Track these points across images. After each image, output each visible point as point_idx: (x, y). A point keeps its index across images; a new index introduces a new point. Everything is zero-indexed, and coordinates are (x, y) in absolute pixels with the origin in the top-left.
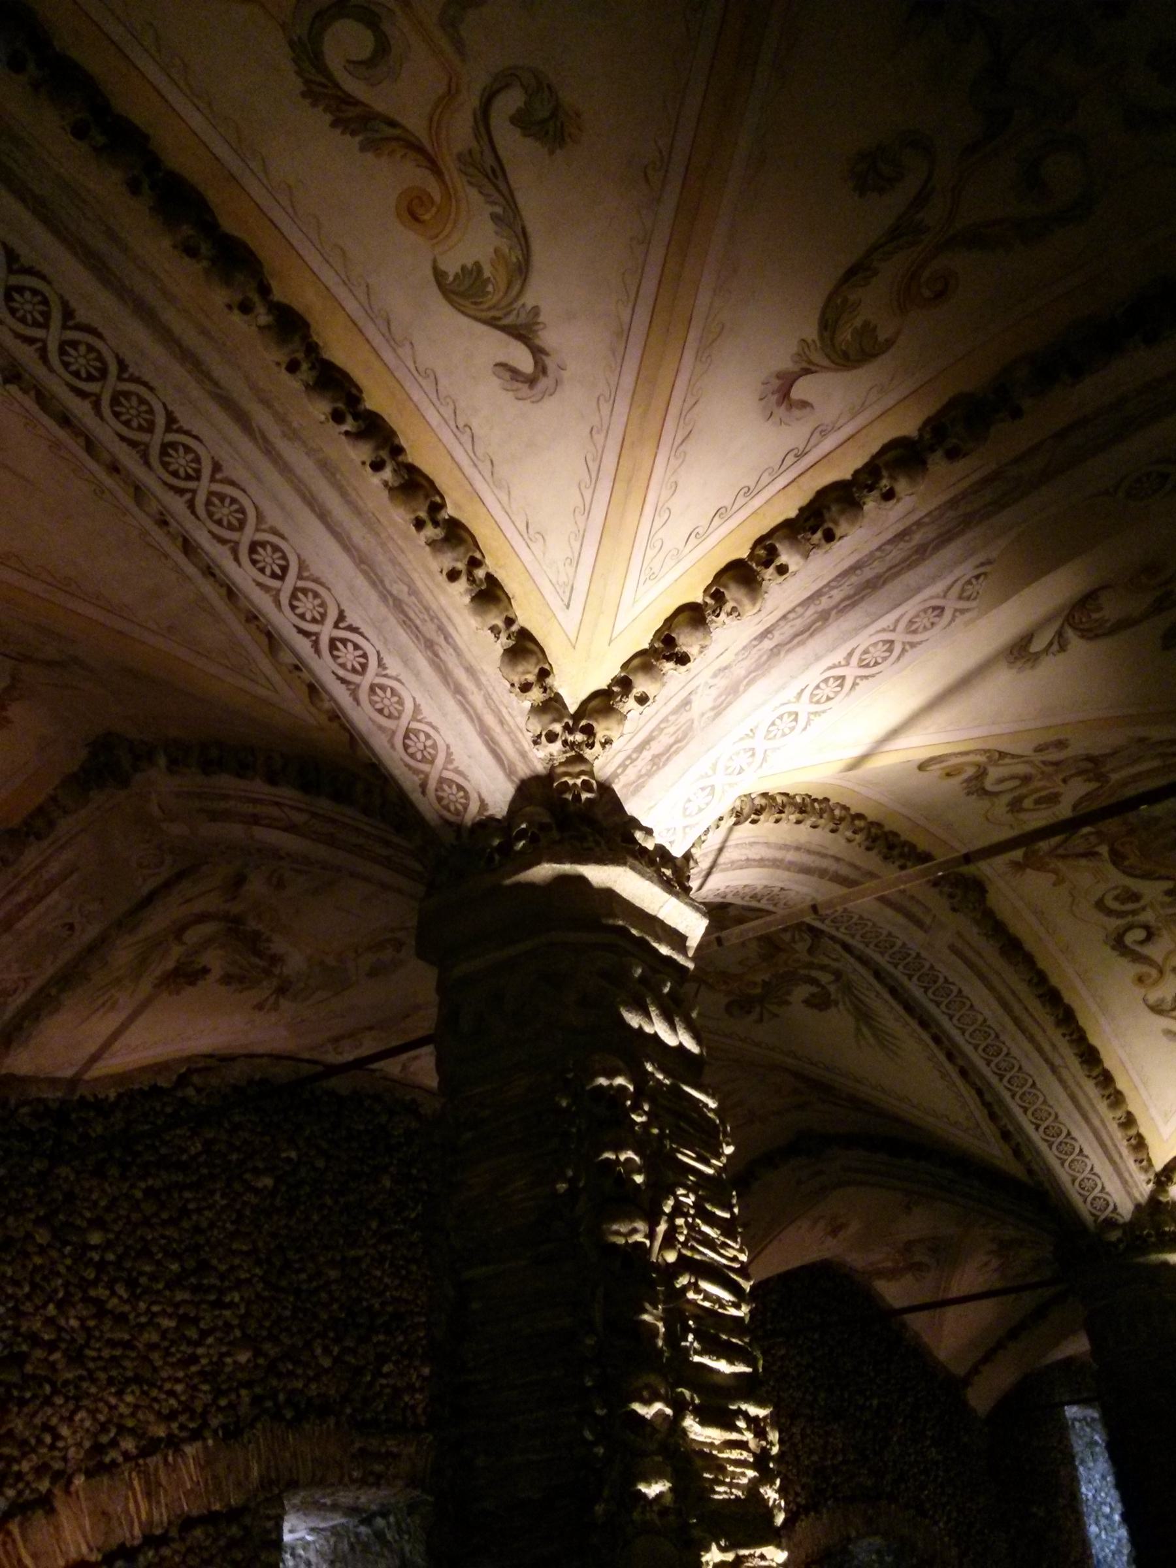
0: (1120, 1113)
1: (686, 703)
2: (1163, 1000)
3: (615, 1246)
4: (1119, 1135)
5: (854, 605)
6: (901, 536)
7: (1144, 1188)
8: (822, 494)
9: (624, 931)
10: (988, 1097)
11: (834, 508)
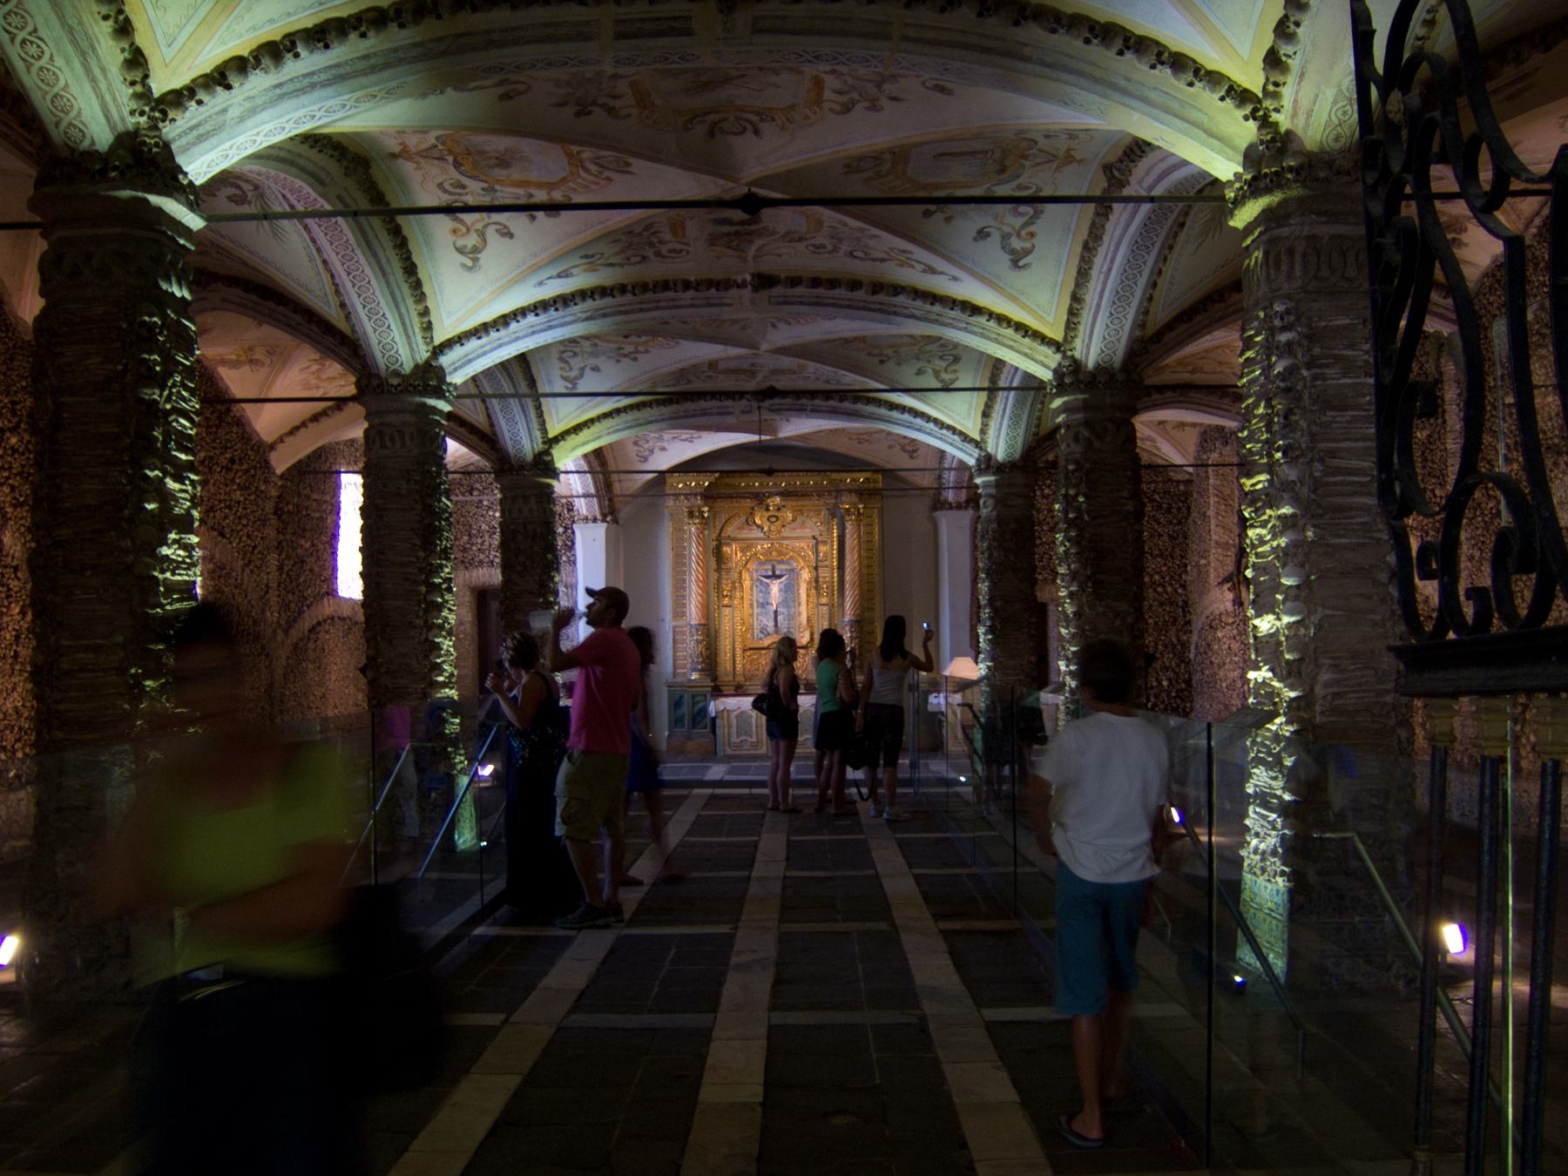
0: (420, 308)
1: (225, 110)
2: (465, 246)
3: (144, 399)
4: (416, 319)
5: (330, 85)
6: (365, 57)
7: (423, 354)
8: (328, 22)
9: (164, 233)
10: (337, 281)
11: (333, 34)
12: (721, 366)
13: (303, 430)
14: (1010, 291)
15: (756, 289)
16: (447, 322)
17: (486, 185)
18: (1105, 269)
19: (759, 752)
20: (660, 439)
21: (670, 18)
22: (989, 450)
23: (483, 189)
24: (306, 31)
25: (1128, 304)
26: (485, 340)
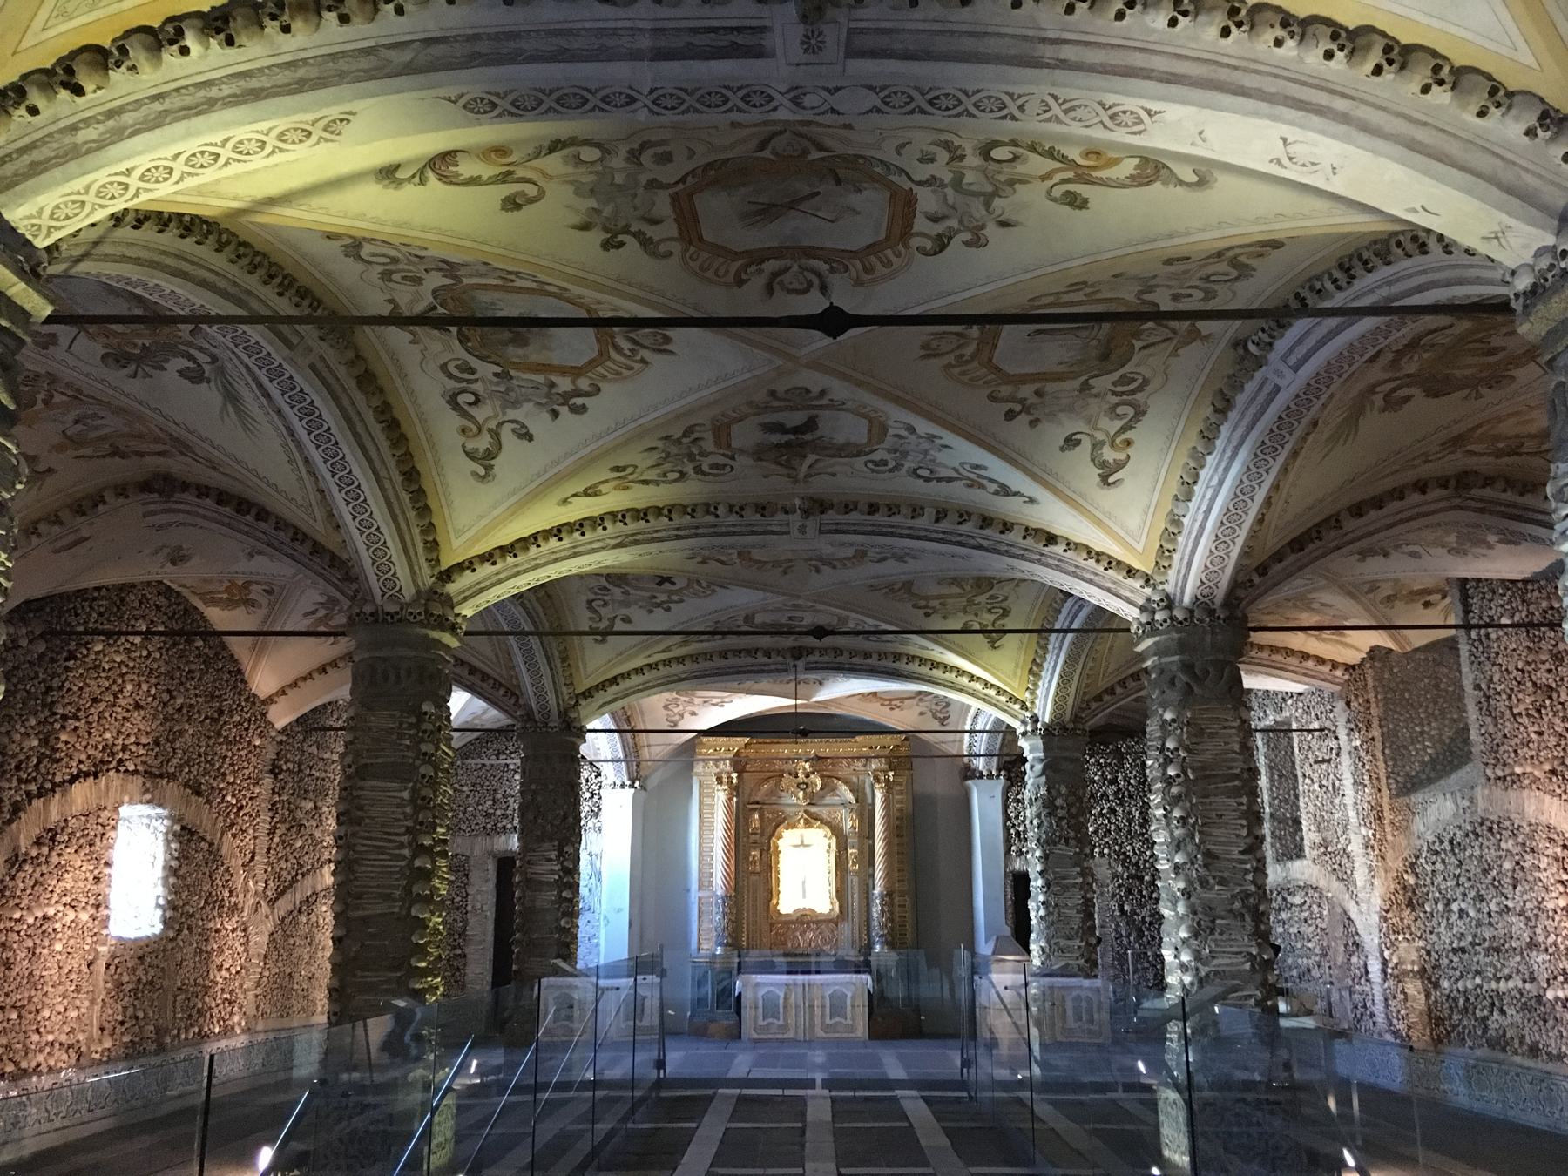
0: (426, 522)
5: (237, 104)
7: (427, 579)
11: (239, 19)
12: (759, 619)
13: (309, 682)
14: (1097, 514)
15: (806, 513)
16: (456, 543)
17: (499, 370)
18: (1215, 482)
19: (786, 1036)
20: (691, 702)
21: (732, 29)
22: (1036, 711)
23: (496, 375)
24: (199, 15)
25: (1239, 525)
26: (498, 567)
